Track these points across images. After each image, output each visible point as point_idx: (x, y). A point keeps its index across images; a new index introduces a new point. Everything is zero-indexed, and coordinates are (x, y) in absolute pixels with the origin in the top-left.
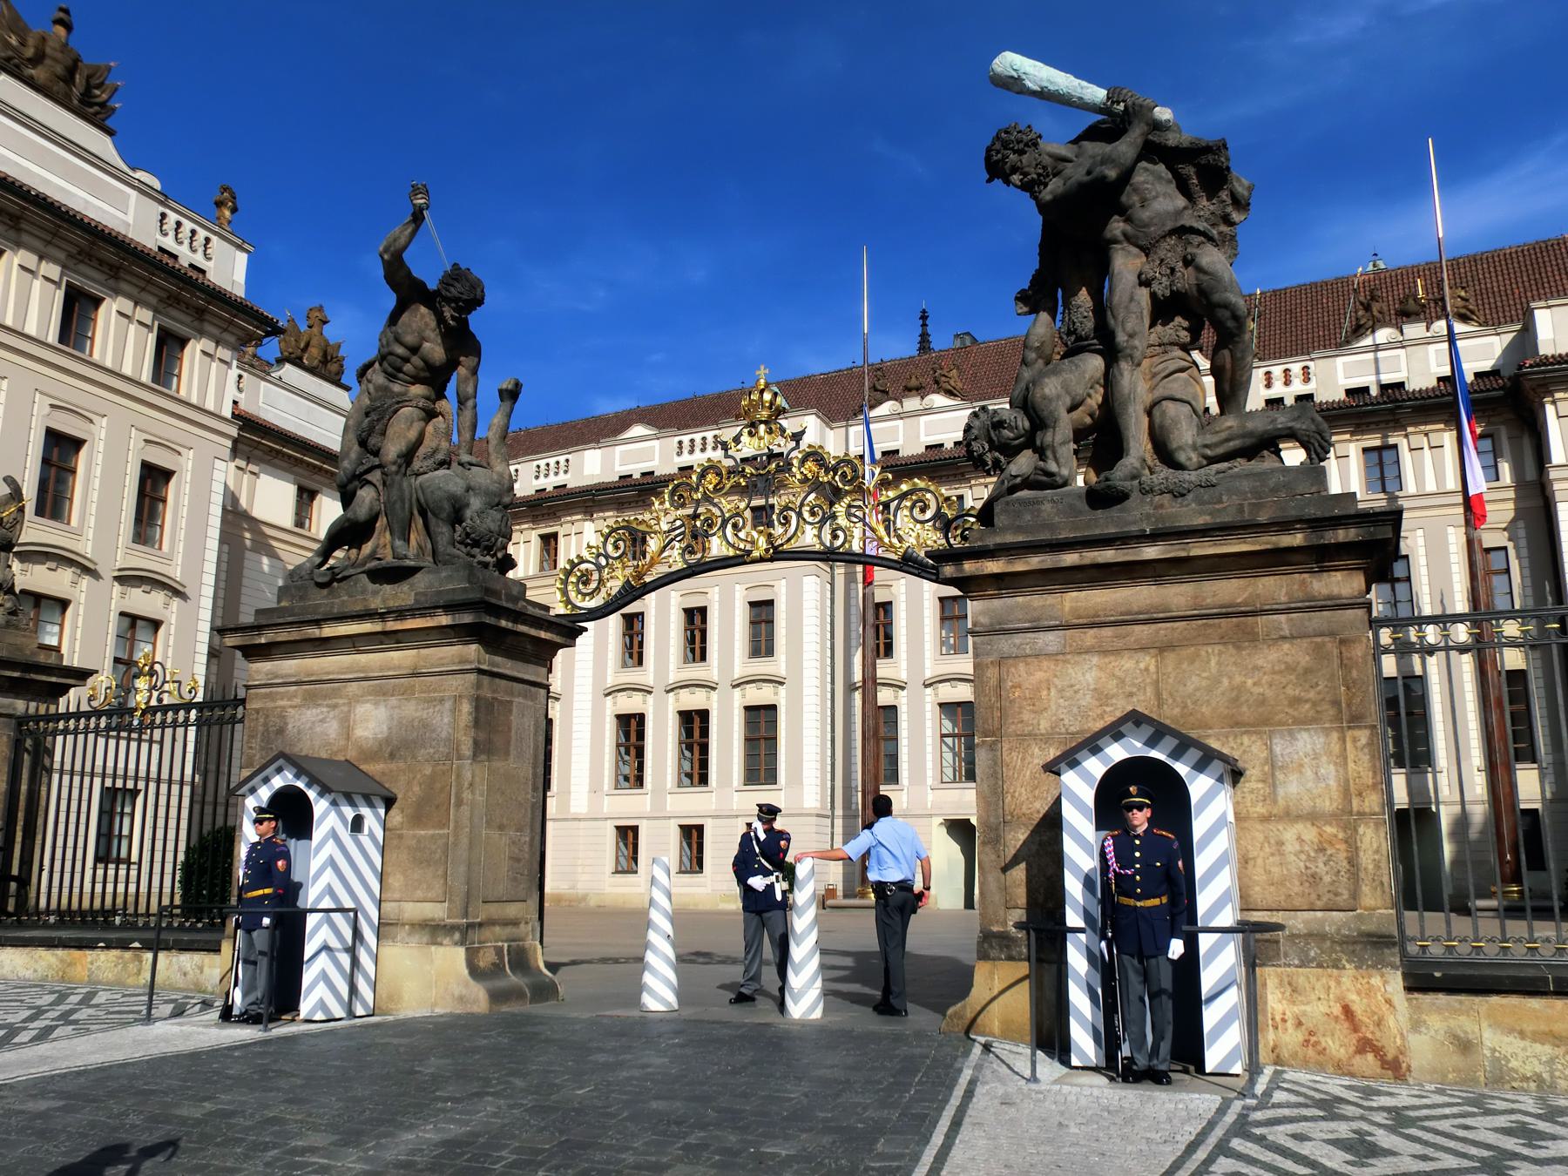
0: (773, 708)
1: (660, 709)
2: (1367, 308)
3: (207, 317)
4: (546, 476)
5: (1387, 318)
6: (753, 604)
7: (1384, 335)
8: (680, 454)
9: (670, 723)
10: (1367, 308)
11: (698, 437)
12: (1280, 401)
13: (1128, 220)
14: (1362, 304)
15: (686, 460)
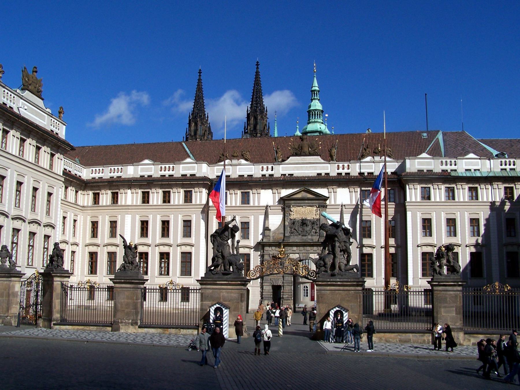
0: (190, 253)
1: (153, 252)
2: (365, 150)
3: (61, 148)
4: (114, 172)
5: (371, 154)
6: (184, 221)
7: (369, 159)
8: (161, 171)
9: (157, 256)
10: (365, 150)
11: (167, 166)
12: (341, 174)
13: (338, 239)
14: (364, 148)
15: (163, 173)
